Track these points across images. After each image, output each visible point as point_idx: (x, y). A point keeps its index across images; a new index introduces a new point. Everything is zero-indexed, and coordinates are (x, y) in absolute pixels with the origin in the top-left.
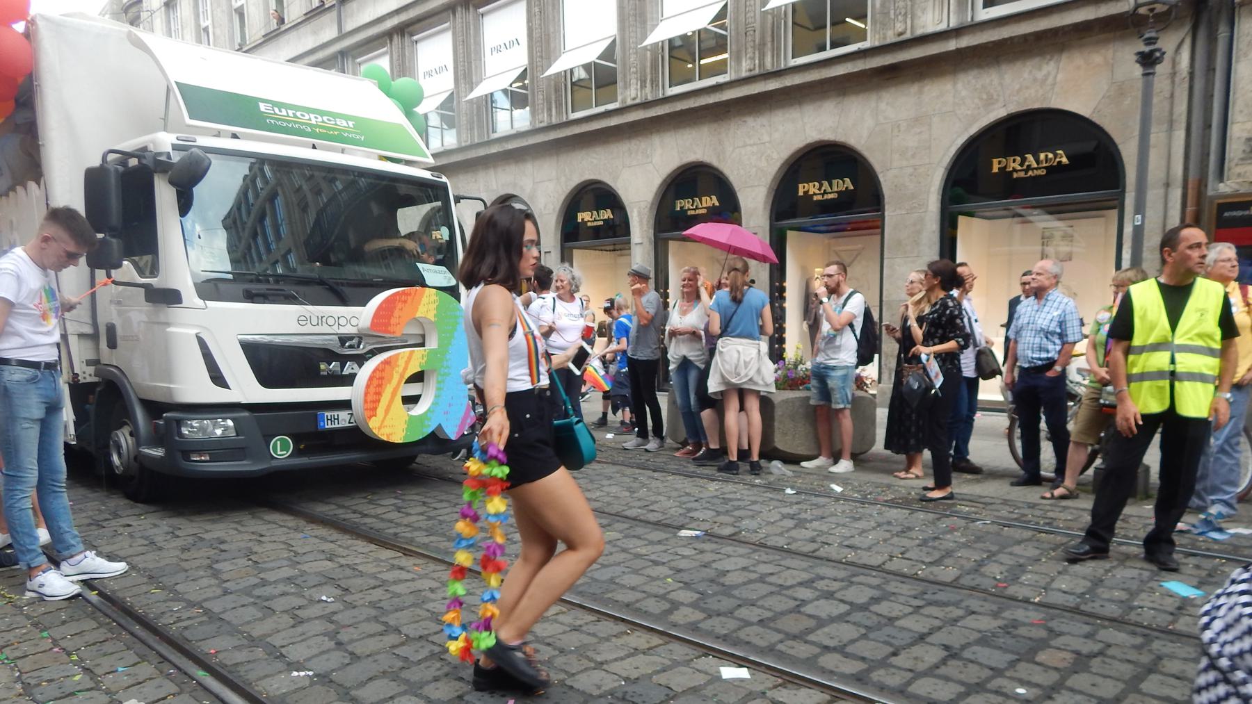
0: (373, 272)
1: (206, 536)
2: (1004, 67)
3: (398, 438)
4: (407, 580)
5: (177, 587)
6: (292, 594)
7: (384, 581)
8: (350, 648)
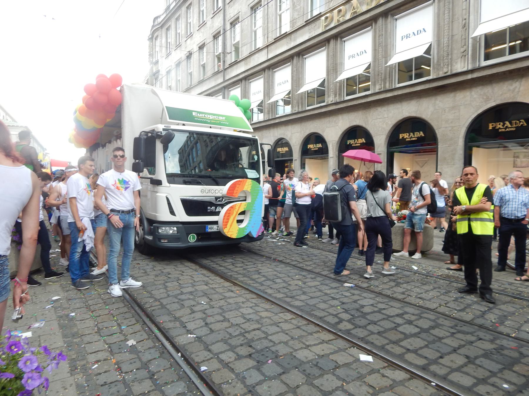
0: (228, 172)
1: (164, 271)
2: (494, 85)
3: (234, 236)
4: (234, 297)
5: (152, 292)
6: (192, 299)
7: (225, 297)
8: (210, 326)
